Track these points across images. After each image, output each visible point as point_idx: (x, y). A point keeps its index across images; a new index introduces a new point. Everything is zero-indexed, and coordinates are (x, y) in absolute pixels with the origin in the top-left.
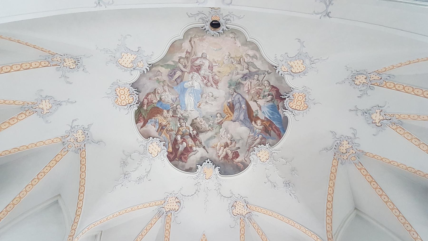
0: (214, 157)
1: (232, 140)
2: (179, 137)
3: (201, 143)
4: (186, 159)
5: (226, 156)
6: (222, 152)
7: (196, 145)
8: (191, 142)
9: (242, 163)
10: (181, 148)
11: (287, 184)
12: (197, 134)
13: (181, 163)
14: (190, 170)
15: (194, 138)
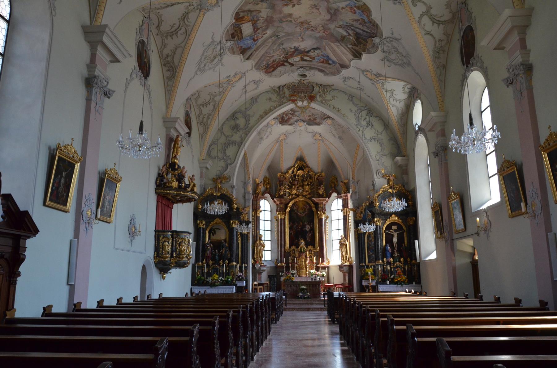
0: (303, 119)
1: (313, 114)
2: (284, 116)
3: (296, 115)
4: (289, 121)
5: (310, 119)
6: (308, 118)
7: (293, 116)
8: (290, 116)
9: (318, 122)
10: (286, 119)
11: (340, 138)
12: (294, 113)
13: (286, 123)
14: (291, 124)
15: (292, 114)
